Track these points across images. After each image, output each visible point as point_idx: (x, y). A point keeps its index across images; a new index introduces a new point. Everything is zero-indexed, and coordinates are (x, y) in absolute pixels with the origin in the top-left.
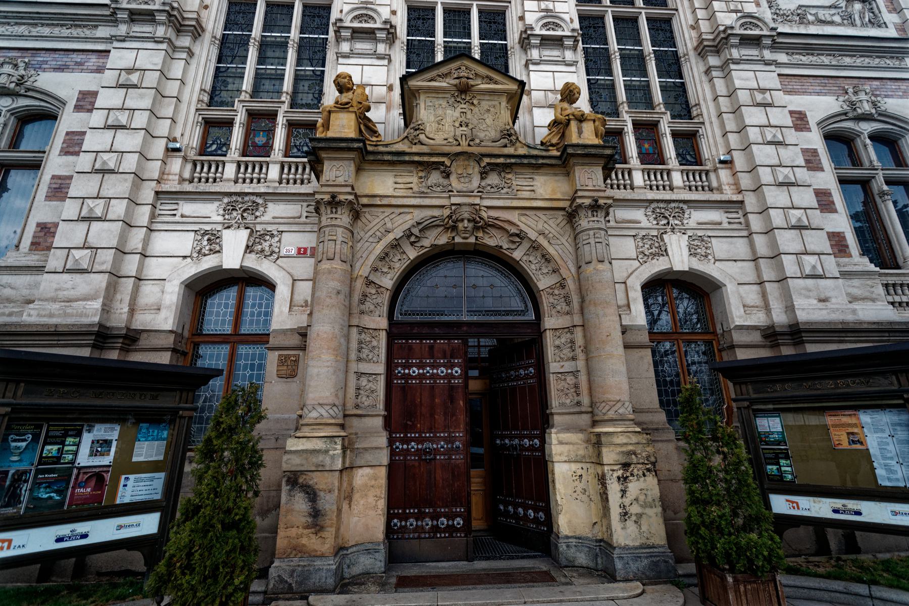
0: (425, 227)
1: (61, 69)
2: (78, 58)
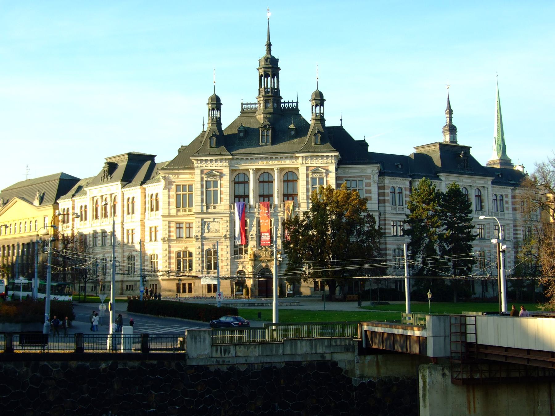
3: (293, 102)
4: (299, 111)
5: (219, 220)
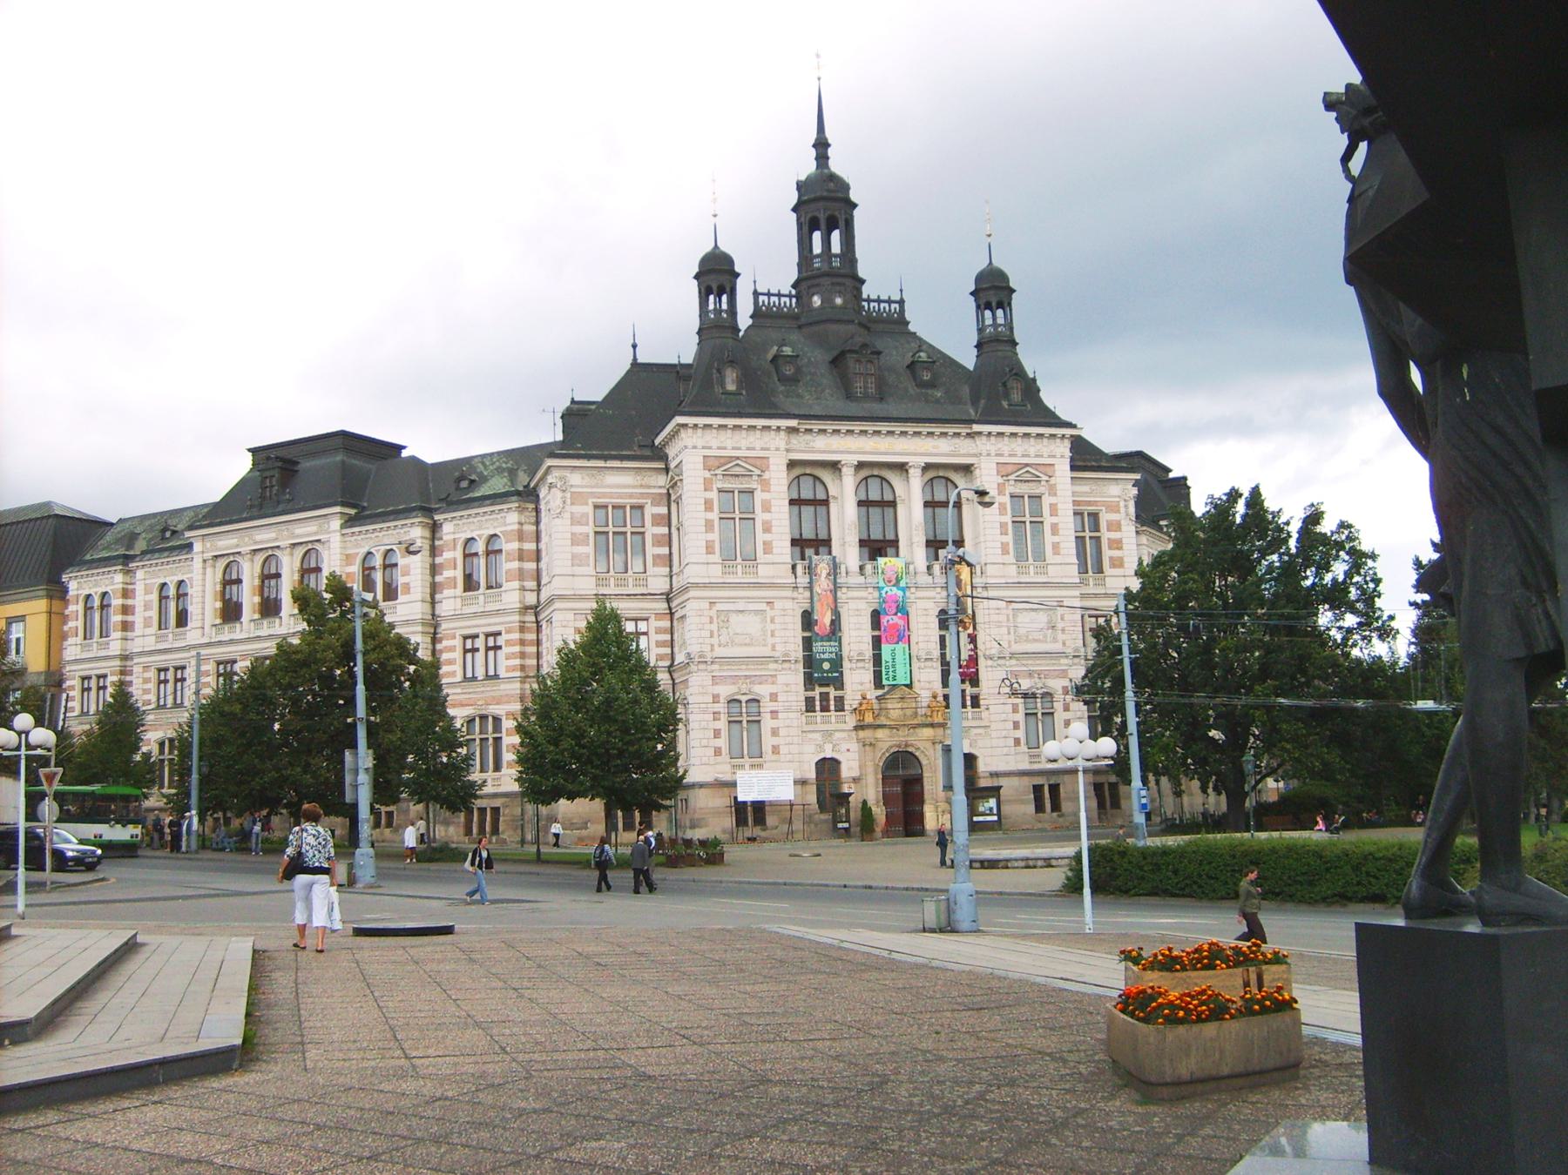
0: (891, 747)
1: (760, 683)
2: (765, 678)
3: (889, 302)
4: (908, 323)
5: (764, 606)
